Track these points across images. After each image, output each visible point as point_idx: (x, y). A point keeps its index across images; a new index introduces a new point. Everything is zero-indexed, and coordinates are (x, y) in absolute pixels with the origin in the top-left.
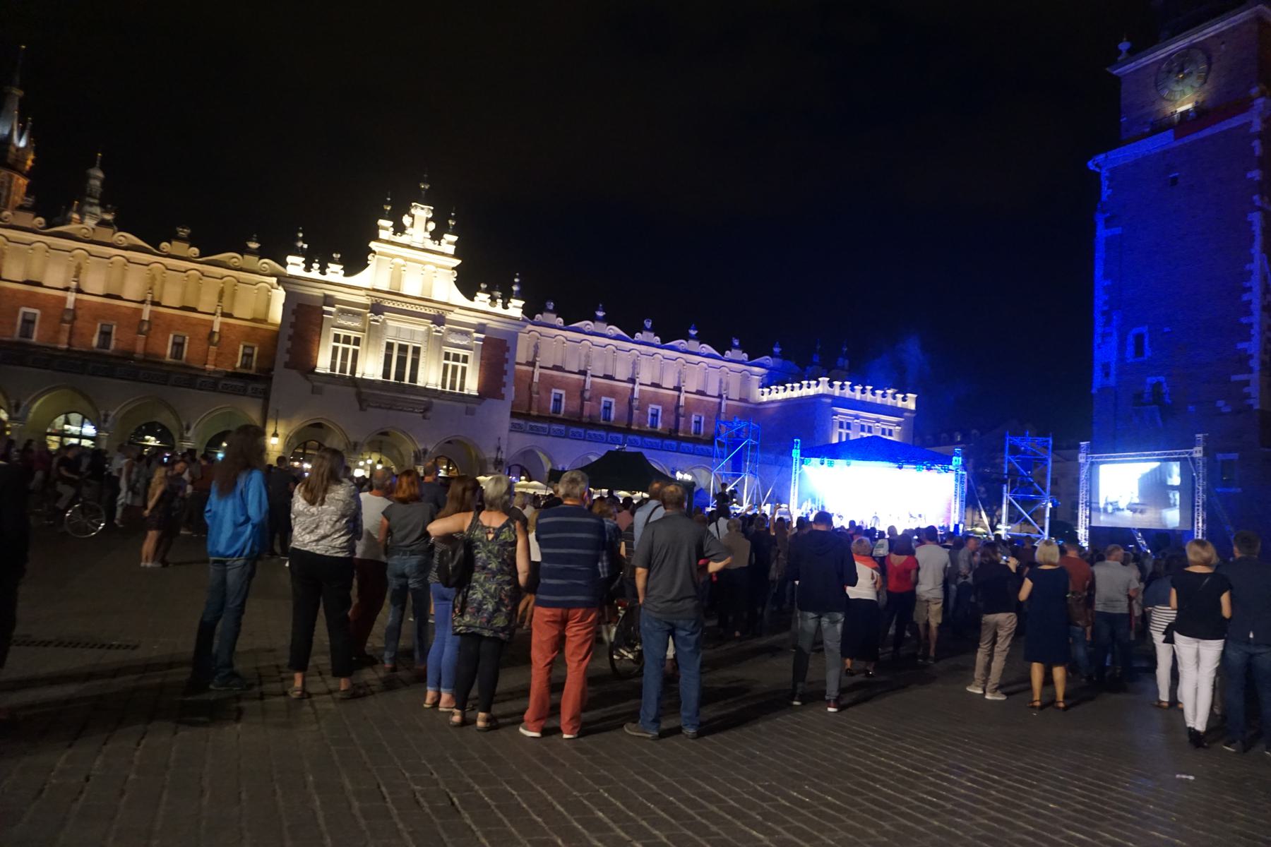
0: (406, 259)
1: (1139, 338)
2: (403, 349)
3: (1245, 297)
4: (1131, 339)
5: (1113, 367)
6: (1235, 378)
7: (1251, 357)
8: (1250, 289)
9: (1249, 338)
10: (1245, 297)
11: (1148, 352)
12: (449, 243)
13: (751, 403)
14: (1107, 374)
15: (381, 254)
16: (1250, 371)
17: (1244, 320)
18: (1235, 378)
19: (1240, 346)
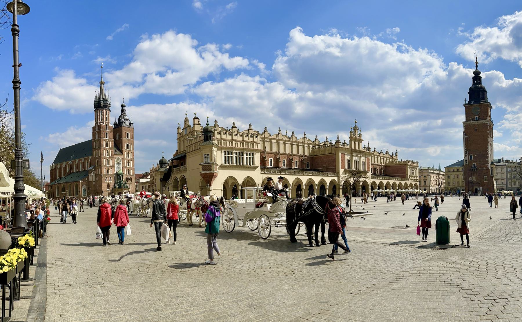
1: (471, 156)
3: (487, 152)
4: (470, 156)
10: (487, 152)
11: (473, 159)
14: (466, 162)
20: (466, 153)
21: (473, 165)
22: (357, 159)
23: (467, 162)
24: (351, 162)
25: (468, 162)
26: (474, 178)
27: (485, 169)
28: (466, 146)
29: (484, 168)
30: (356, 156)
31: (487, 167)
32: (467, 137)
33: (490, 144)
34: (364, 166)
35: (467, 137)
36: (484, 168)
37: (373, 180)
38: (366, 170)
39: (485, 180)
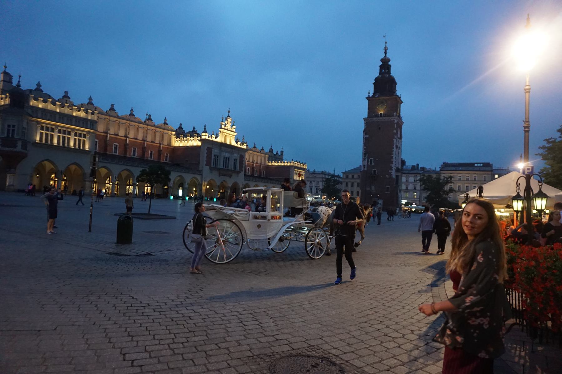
0: (227, 133)
2: (226, 158)
3: (392, 155)
4: (369, 160)
5: (366, 166)
6: (390, 171)
7: (393, 167)
8: (393, 154)
9: (392, 164)
10: (392, 155)
11: (373, 164)
12: (234, 128)
13: (172, 146)
14: (365, 168)
15: (223, 132)
16: (392, 170)
17: (392, 160)
18: (390, 171)
19: (391, 165)
20: (365, 156)
21: (373, 172)
22: (227, 155)
23: (366, 167)
24: (219, 158)
25: (367, 168)
26: (373, 187)
27: (388, 177)
28: (365, 147)
29: (387, 176)
30: (226, 152)
31: (390, 174)
32: (368, 136)
33: (397, 147)
34: (235, 164)
35: (368, 136)
36: (387, 176)
37: (246, 182)
38: (238, 168)
39: (387, 191)
